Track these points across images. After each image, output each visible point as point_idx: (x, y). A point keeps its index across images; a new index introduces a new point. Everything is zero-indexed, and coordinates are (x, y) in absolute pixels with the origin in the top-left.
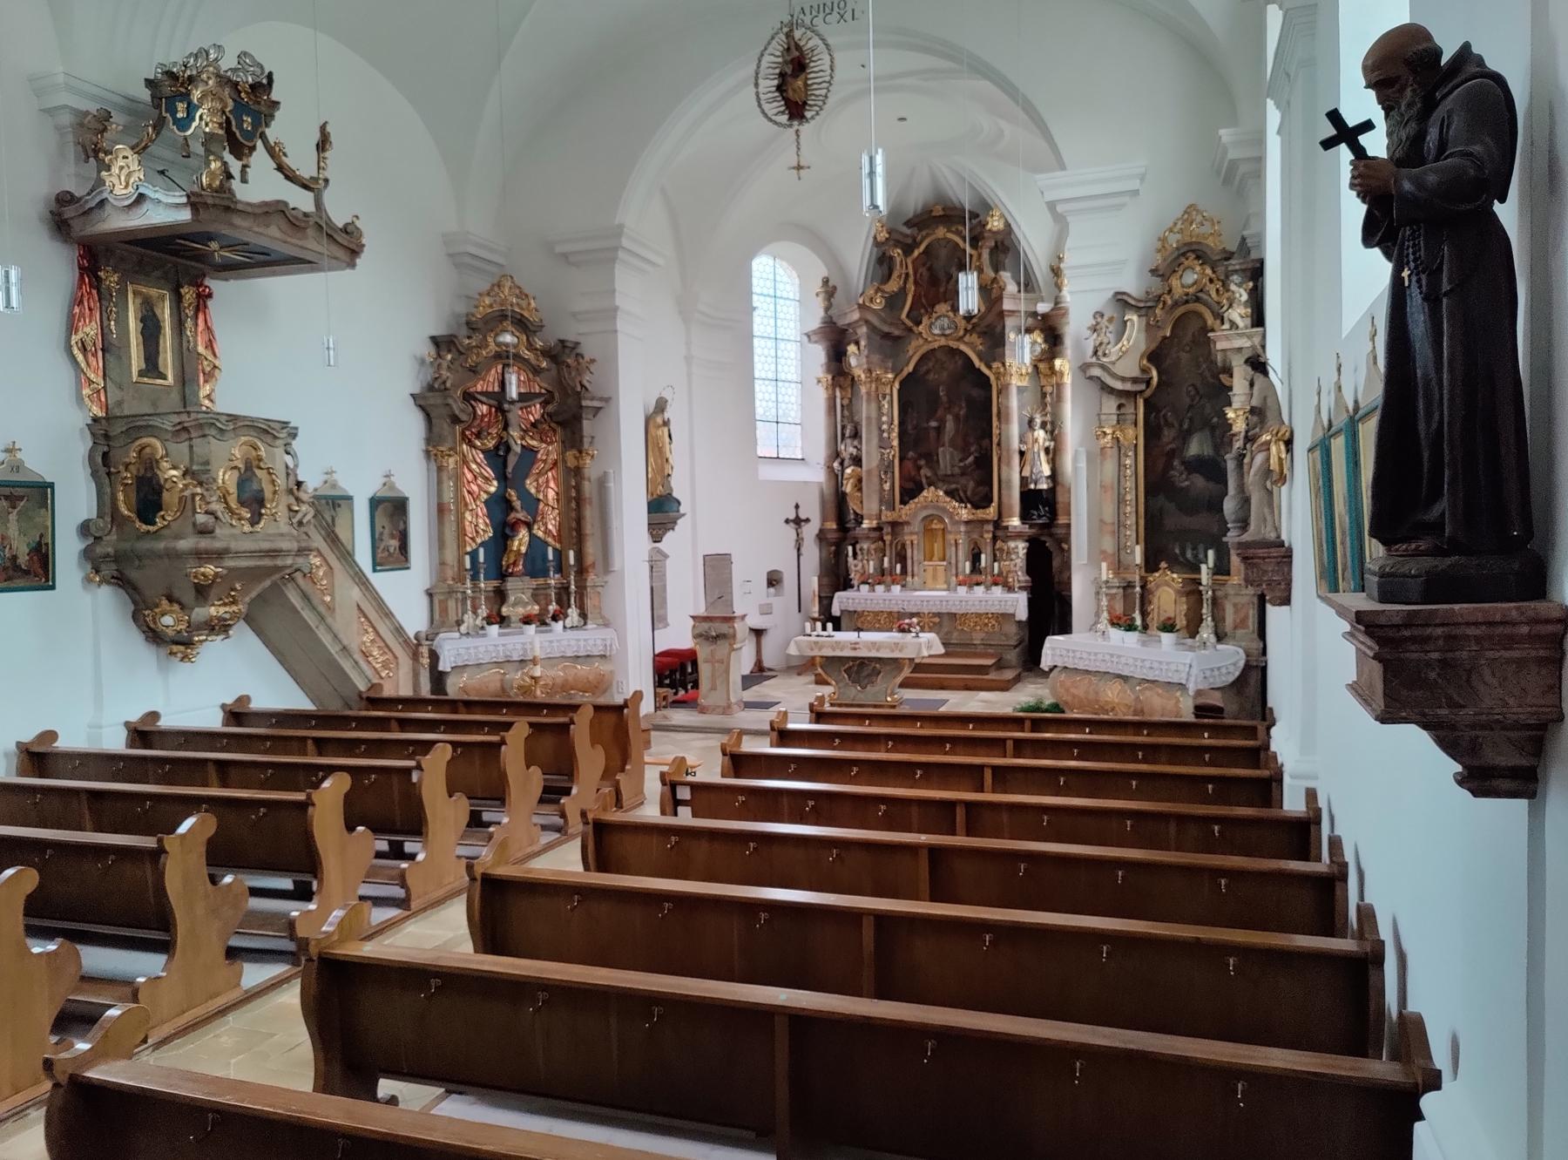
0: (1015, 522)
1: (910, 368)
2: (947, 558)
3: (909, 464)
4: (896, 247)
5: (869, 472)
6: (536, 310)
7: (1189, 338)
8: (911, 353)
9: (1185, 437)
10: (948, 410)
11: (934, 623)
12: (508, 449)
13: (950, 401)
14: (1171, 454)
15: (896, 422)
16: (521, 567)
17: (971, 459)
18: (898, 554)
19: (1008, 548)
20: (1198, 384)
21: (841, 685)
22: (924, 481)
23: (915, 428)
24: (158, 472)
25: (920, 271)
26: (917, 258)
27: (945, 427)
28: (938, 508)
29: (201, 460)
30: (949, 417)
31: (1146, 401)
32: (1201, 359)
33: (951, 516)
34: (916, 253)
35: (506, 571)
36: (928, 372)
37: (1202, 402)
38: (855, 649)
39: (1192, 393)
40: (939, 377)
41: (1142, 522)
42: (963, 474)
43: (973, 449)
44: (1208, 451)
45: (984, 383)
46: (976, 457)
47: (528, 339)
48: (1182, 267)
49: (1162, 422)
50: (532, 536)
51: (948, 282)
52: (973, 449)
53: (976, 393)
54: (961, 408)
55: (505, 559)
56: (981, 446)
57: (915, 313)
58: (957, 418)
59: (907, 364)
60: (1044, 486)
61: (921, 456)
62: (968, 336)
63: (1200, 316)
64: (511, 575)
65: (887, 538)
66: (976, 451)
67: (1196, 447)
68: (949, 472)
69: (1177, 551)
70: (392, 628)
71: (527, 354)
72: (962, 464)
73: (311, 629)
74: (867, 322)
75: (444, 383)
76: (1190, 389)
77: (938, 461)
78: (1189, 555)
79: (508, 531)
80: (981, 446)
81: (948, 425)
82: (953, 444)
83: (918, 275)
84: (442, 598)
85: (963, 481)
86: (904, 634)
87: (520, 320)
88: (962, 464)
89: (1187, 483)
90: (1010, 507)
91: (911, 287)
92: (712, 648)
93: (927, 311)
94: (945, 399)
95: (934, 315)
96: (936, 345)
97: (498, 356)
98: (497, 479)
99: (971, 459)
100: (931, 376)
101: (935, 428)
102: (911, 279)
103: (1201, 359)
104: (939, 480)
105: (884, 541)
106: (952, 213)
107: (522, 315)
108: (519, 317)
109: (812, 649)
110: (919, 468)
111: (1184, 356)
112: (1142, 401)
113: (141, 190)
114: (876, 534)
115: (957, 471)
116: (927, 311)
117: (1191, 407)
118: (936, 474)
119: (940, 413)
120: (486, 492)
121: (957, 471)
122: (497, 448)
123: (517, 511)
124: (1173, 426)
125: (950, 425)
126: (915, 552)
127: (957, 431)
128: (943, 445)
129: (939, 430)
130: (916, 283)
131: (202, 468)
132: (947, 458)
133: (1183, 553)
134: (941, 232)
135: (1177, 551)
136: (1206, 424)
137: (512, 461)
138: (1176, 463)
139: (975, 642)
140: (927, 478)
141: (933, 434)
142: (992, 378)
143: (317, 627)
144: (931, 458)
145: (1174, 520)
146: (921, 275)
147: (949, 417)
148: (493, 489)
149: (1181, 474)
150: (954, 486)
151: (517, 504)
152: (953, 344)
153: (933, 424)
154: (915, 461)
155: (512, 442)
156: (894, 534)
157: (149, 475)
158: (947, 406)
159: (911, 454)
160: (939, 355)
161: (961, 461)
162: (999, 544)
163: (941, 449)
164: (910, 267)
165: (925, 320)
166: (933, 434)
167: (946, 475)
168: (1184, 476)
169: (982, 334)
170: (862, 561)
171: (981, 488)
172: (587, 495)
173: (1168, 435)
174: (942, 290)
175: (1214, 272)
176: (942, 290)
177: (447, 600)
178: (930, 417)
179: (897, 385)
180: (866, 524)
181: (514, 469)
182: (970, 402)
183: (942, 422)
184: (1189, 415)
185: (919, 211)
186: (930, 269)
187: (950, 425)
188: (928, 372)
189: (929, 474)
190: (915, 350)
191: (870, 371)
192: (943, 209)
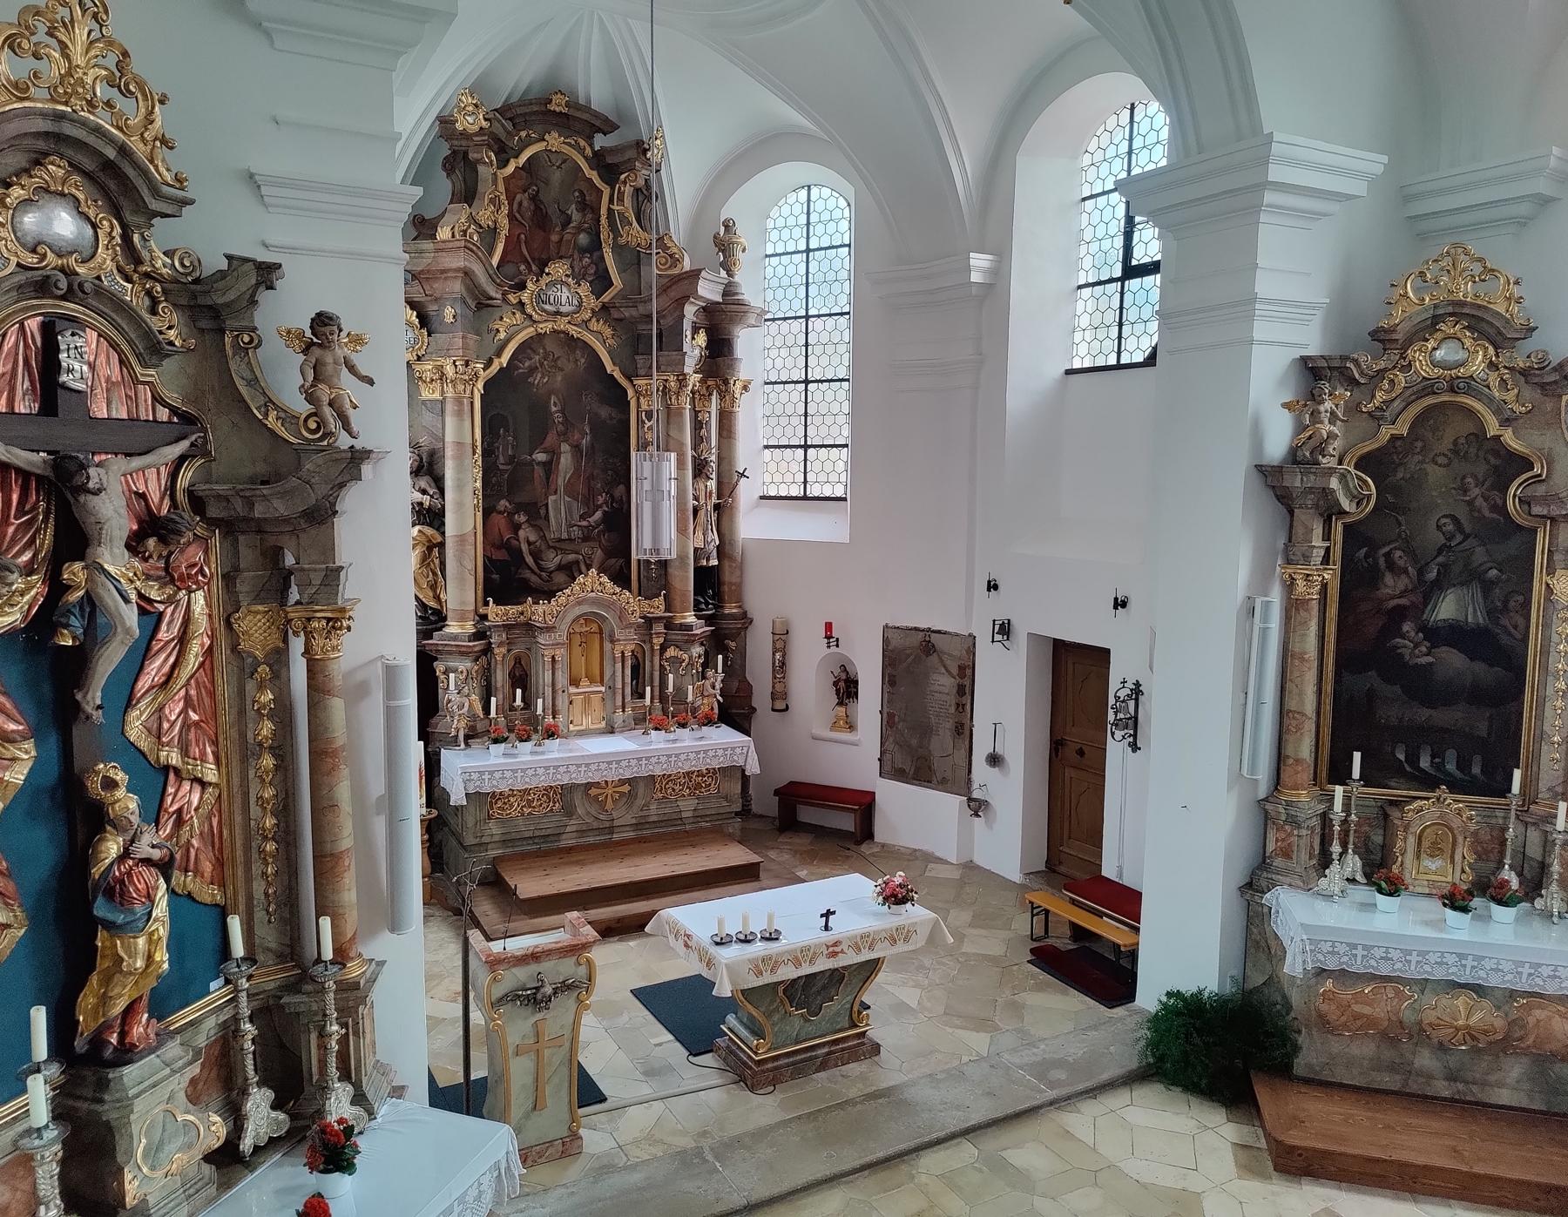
0: (690, 618)
1: (505, 359)
2: (606, 678)
3: (499, 521)
4: (490, 147)
5: (461, 539)
6: (164, 142)
7: (1446, 444)
8: (502, 335)
9: (1430, 591)
10: (564, 436)
11: (622, 794)
13: (566, 422)
14: (1399, 614)
15: (479, 451)
17: (598, 514)
18: (512, 675)
19: (691, 658)
20: (1462, 514)
21: (776, 1017)
22: (524, 547)
23: (511, 460)
25: (518, 197)
26: (513, 175)
27: (558, 463)
28: (595, 602)
30: (565, 447)
31: (1346, 527)
32: (1469, 480)
33: (622, 614)
34: (510, 168)
36: (532, 370)
37: (1466, 545)
38: (834, 954)
39: (1450, 527)
40: (550, 382)
41: (1328, 707)
42: (586, 539)
43: (601, 500)
44: (1475, 616)
45: (619, 400)
46: (605, 513)
48: (1439, 335)
49: (1382, 561)
51: (563, 230)
52: (601, 500)
53: (604, 412)
54: (584, 434)
55: (87, 1000)
56: (612, 496)
57: (510, 269)
58: (576, 448)
59: (499, 355)
60: (714, 562)
61: (519, 508)
62: (594, 320)
63: (1470, 413)
65: (499, 651)
66: (606, 503)
67: (1447, 608)
68: (564, 536)
69: (1402, 757)
71: (129, 292)
72: (584, 523)
74: (467, 274)
76: (1444, 521)
77: (547, 517)
78: (1425, 763)
80: (612, 496)
81: (562, 460)
82: (570, 490)
83: (515, 206)
85: (585, 549)
86: (902, 908)
87: (108, 166)
88: (584, 523)
89: (1430, 659)
90: (684, 594)
91: (504, 222)
92: (539, 1016)
93: (530, 270)
94: (558, 418)
95: (545, 280)
96: (546, 327)
98: (35, 733)
99: (598, 514)
100: (537, 379)
101: (544, 464)
102: (505, 210)
103: (1469, 480)
104: (550, 547)
105: (487, 650)
106: (578, 114)
109: (759, 973)
110: (516, 528)
111: (1435, 473)
112: (1340, 528)
114: (478, 645)
115: (576, 532)
116: (530, 270)
117: (1440, 551)
118: (544, 538)
119: (551, 439)
121: (576, 532)
122: (45, 620)
124: (1406, 571)
125: (566, 460)
126: (559, 674)
127: (577, 470)
128: (556, 493)
129: (549, 467)
130: (511, 216)
132: (561, 511)
133: (1413, 759)
134: (554, 141)
135: (1402, 757)
136: (1472, 576)
137: (109, 660)
138: (1407, 627)
139: (684, 815)
140: (529, 543)
141: (539, 471)
142: (630, 393)
144: (536, 513)
145: (1395, 709)
146: (520, 204)
147: (565, 447)
149: (1416, 646)
150: (572, 557)
151: (127, 803)
152: (574, 331)
153: (541, 457)
154: (511, 515)
156: (510, 643)
158: (561, 428)
159: (503, 504)
160: (550, 346)
161: (582, 517)
162: (671, 652)
163: (552, 498)
164: (501, 187)
165: (530, 285)
166: (539, 472)
167: (560, 540)
168: (1424, 649)
169: (616, 323)
170: (468, 696)
171: (614, 560)
172: (339, 742)
173: (1392, 586)
174: (554, 238)
175: (1497, 356)
176: (554, 238)
178: (534, 446)
179: (480, 385)
180: (453, 628)
182: (597, 426)
183: (554, 454)
184: (1440, 559)
185: (514, 99)
186: (534, 199)
187: (566, 460)
188: (532, 370)
189: (532, 539)
190: (511, 330)
191: (467, 364)
192: (568, 105)
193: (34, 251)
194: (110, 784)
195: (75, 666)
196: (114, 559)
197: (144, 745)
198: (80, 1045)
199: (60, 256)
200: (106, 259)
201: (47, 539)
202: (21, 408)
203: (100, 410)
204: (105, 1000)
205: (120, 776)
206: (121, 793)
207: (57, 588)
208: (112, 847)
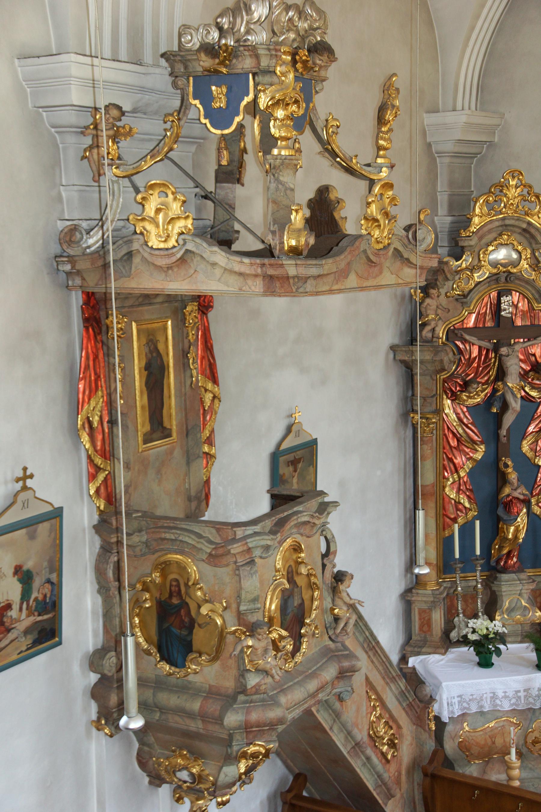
12: (505, 407)
16: (515, 559)
24: (188, 600)
29: (251, 596)
35: (498, 561)
47: (533, 253)
50: (529, 513)
64: (505, 570)
70: (396, 692)
73: (325, 731)
75: (433, 330)
79: (501, 511)
84: (424, 606)
87: (525, 230)
97: (494, 278)
107: (529, 223)
108: (524, 226)
113: (190, 246)
120: (471, 458)
122: (489, 402)
123: (511, 484)
131: (252, 606)
137: (509, 419)
143: (331, 728)
148: (479, 456)
151: (513, 476)
155: (510, 398)
157: (175, 601)
177: (431, 610)
181: (508, 430)
193: (496, 267)
194: (507, 466)
195: (498, 419)
196: (512, 382)
197: (530, 454)
198: (493, 563)
199: (504, 267)
200: (524, 264)
201: (493, 373)
202: (489, 324)
203: (519, 322)
204: (501, 548)
205: (509, 463)
206: (510, 470)
207: (495, 390)
208: (507, 490)
